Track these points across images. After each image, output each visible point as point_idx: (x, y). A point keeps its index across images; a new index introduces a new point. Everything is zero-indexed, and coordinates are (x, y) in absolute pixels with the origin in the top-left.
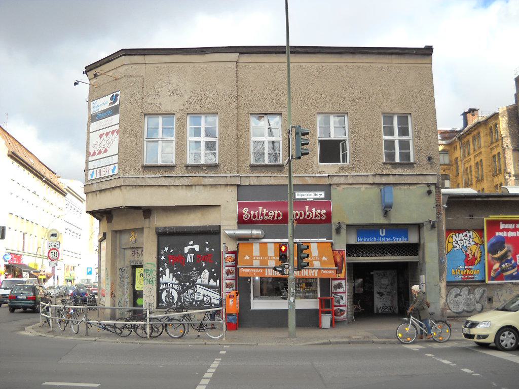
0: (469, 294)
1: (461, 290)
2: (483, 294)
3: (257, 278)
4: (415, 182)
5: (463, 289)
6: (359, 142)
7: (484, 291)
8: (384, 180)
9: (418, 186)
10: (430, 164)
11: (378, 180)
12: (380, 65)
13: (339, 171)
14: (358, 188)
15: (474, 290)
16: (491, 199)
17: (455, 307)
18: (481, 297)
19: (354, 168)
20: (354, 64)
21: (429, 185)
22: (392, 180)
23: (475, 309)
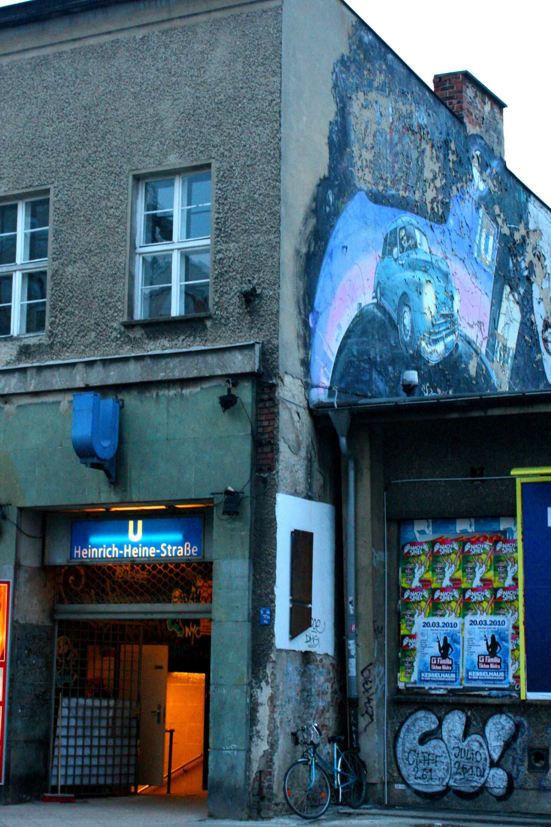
0: (466, 734)
1: (441, 721)
2: (514, 737)
3: (474, 722)
4: (194, 373)
5: (450, 716)
6: (69, 269)
7: (518, 726)
8: (113, 376)
9: (206, 385)
10: (250, 313)
11: (96, 377)
12: (140, 34)
13: (18, 359)
14: (53, 403)
15: (485, 723)
16: (497, 412)
17: (419, 774)
18: (508, 746)
19: (51, 346)
20: (77, 45)
21: (236, 379)
22: (133, 373)
23: (483, 788)
